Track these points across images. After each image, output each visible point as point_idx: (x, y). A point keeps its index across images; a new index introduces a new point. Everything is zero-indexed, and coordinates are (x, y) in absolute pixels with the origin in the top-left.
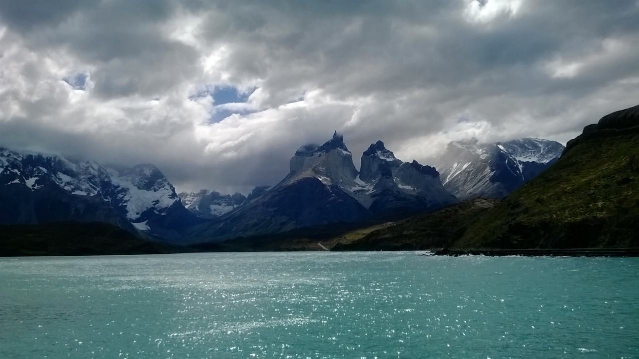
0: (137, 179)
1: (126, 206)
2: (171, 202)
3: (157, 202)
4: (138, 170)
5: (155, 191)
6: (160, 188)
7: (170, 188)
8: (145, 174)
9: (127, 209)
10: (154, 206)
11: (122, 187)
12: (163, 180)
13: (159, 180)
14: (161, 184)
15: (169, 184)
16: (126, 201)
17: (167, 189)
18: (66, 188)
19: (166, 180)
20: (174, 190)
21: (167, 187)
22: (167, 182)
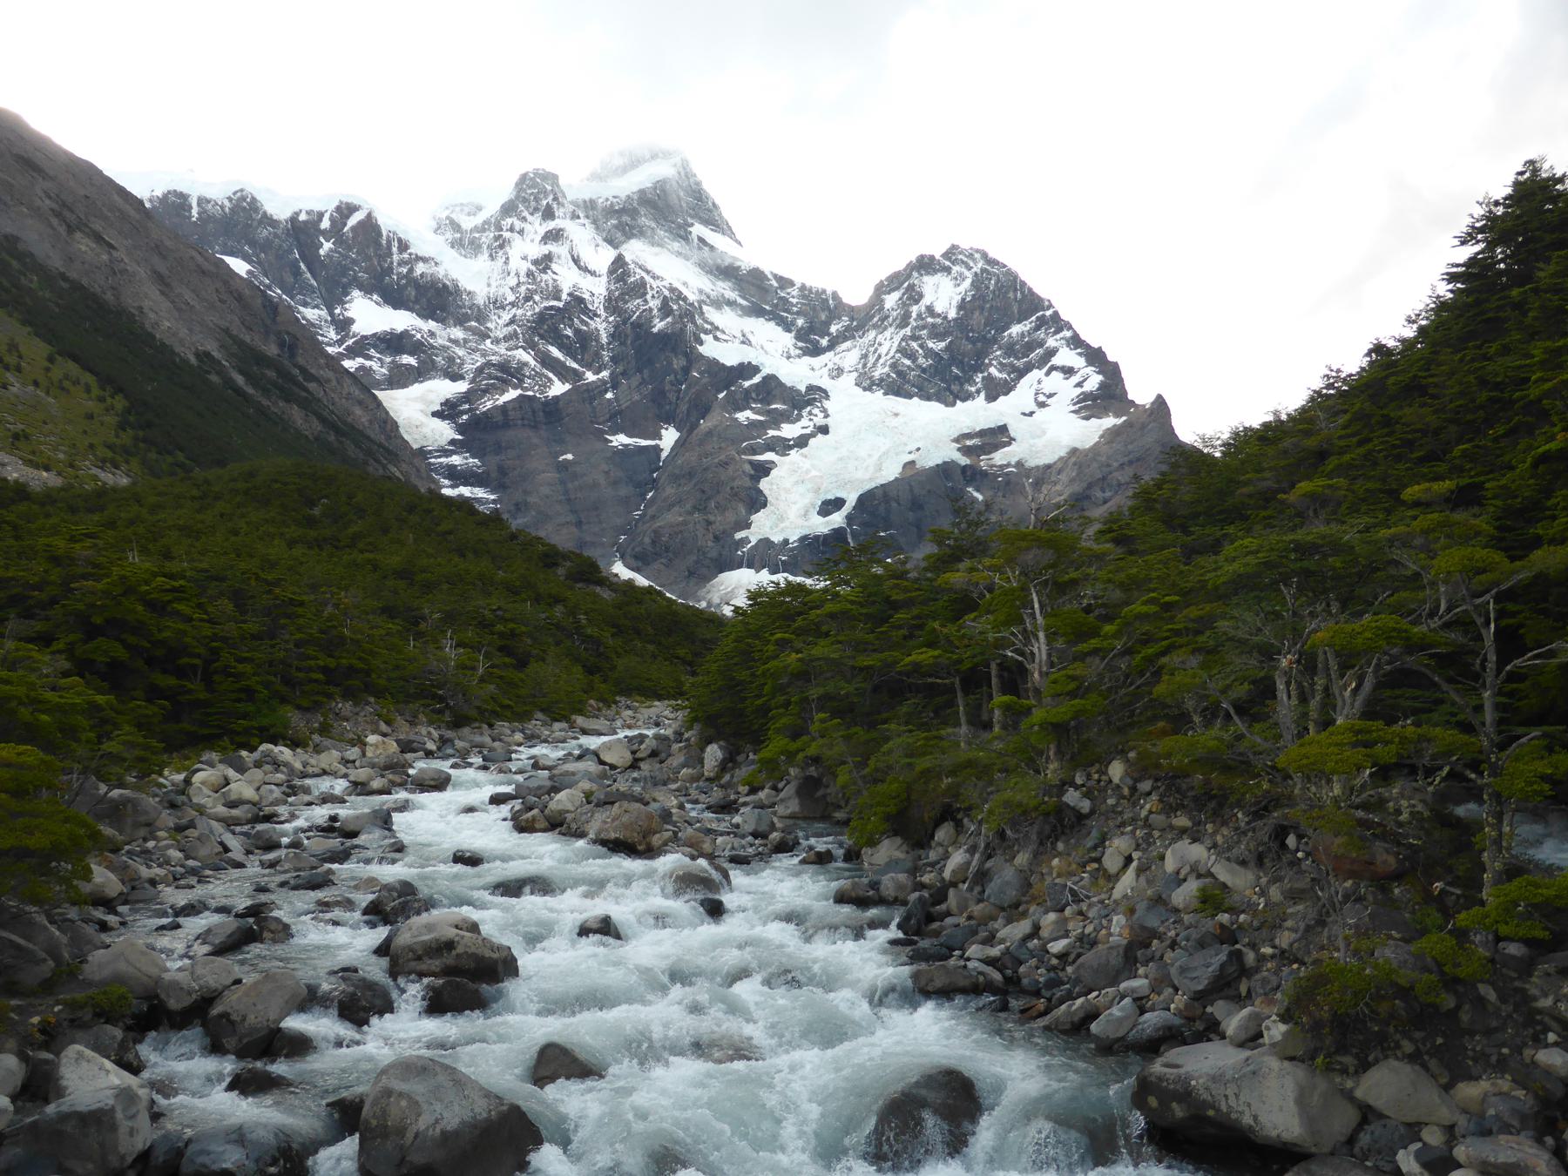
0: (888, 342)
1: (764, 470)
2: (1089, 432)
3: (997, 436)
4: (891, 300)
5: (991, 398)
6: (1022, 373)
7: (1090, 362)
8: (930, 310)
9: (764, 484)
10: (964, 461)
11: (765, 372)
12: (1042, 323)
13: (1016, 330)
14: (1030, 347)
15: (1076, 342)
16: (783, 446)
17: (1068, 371)
18: (347, 364)
19: (1057, 323)
20: (1111, 373)
21: (1067, 357)
22: (1068, 334)
